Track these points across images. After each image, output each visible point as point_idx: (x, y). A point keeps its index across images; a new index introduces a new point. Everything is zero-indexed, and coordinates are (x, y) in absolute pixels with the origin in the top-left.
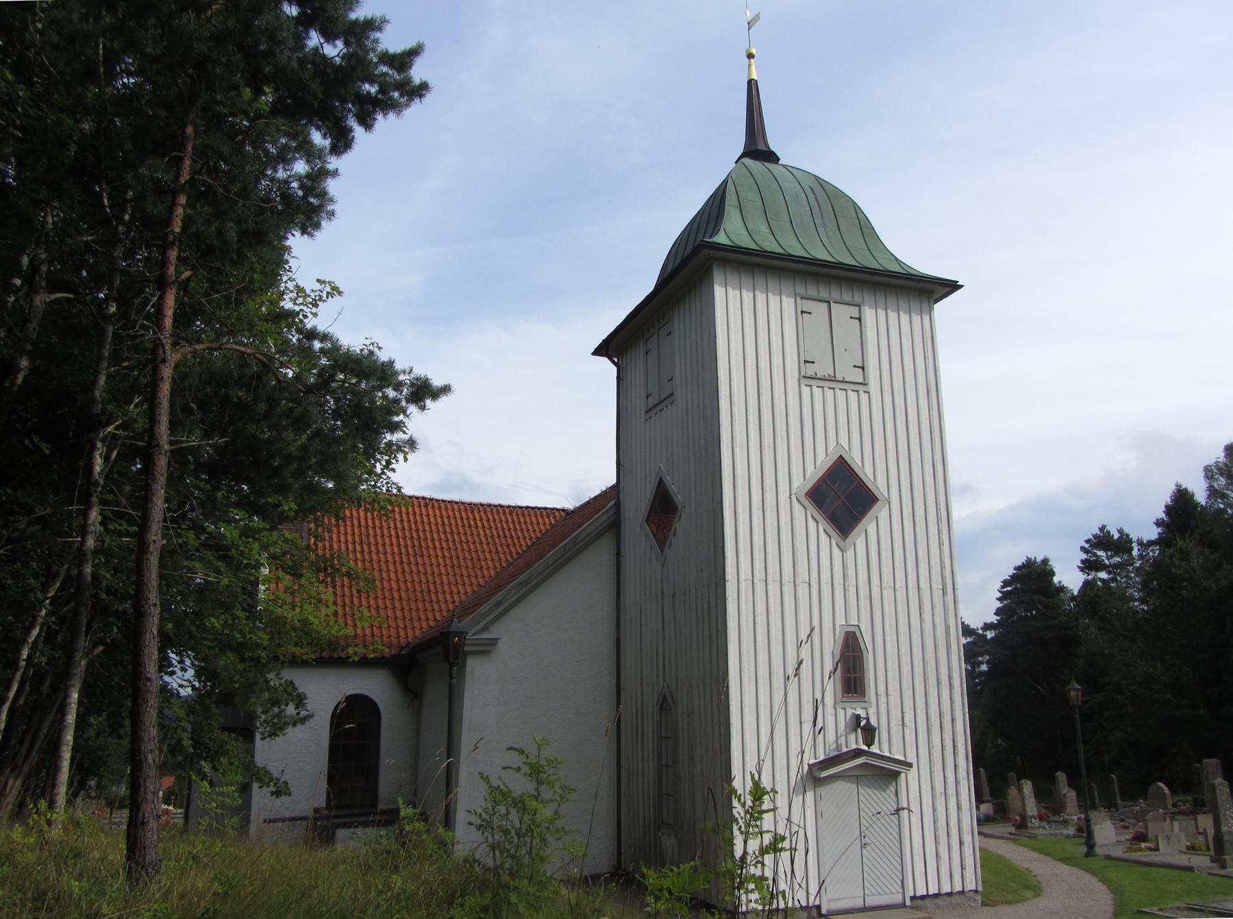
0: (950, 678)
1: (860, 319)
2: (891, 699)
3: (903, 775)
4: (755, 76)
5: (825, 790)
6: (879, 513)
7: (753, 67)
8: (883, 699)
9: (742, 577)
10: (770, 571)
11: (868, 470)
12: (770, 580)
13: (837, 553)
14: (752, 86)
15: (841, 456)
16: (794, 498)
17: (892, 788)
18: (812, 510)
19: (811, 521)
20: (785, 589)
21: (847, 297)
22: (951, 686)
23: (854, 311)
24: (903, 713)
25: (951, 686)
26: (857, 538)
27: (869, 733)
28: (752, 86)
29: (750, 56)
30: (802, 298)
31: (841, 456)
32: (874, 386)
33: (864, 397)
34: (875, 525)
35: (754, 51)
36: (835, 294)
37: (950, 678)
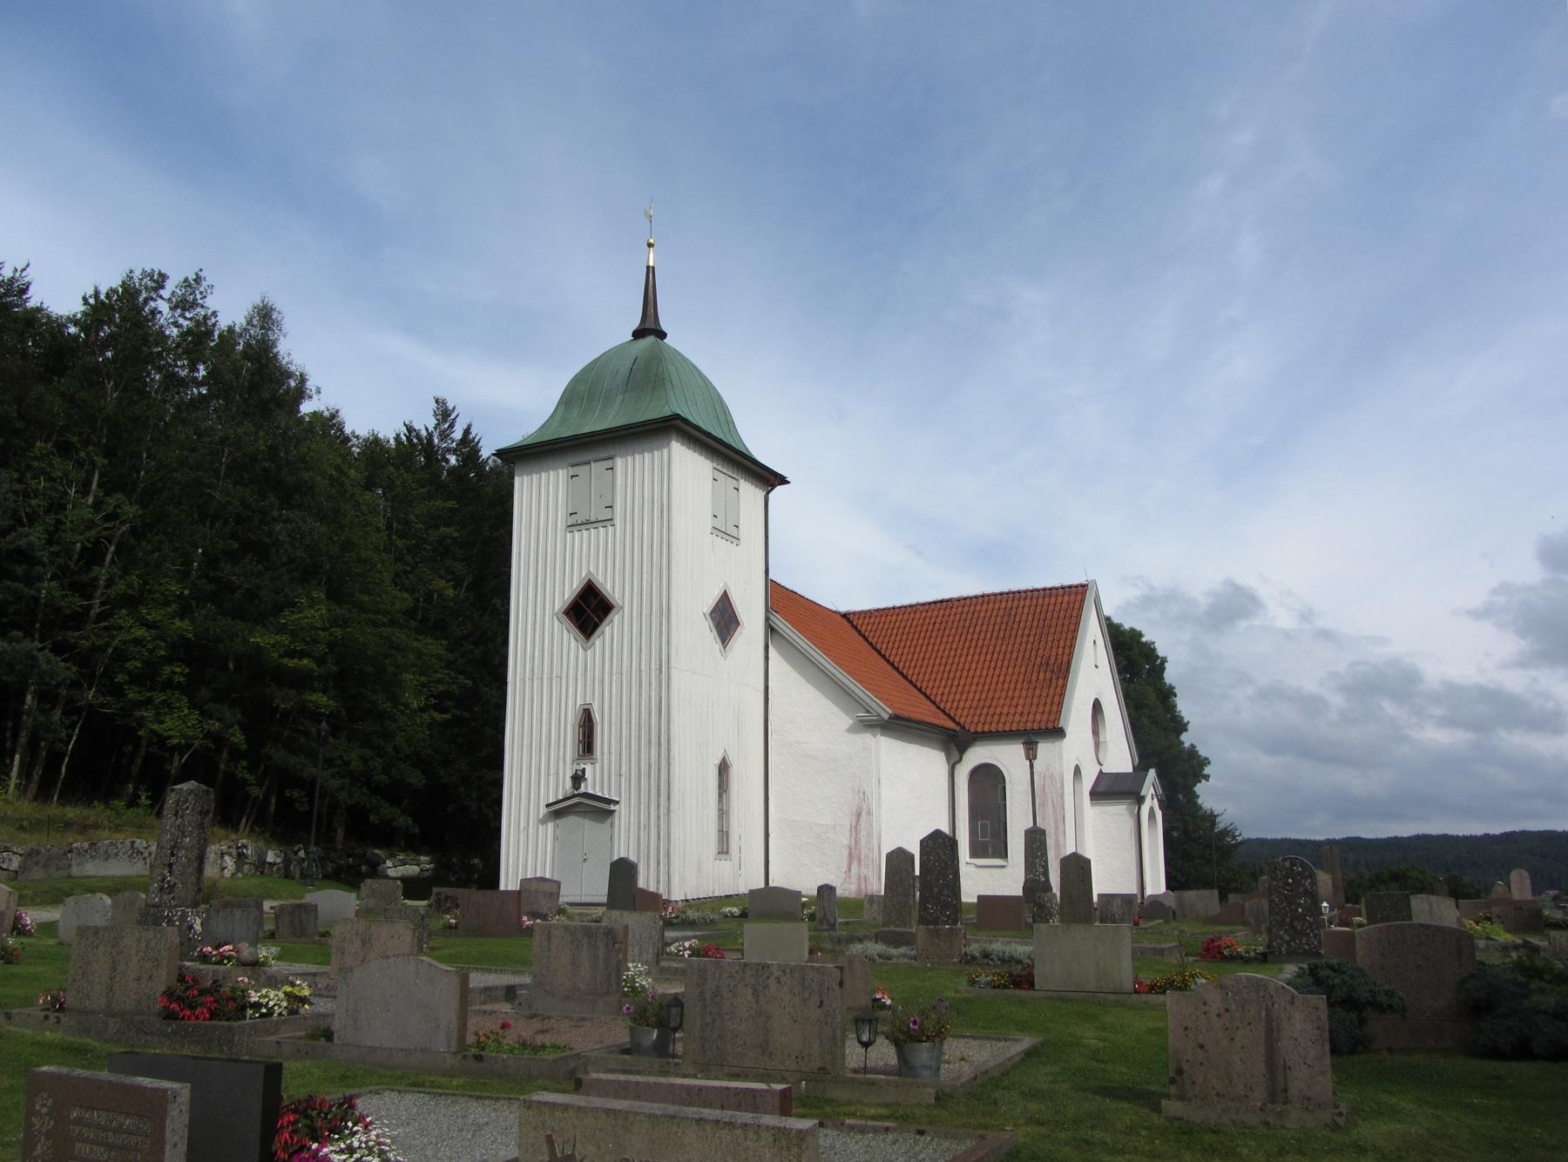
0: (659, 738)
1: (612, 469)
2: (613, 756)
3: (617, 813)
4: (651, 264)
5: (563, 822)
6: (615, 617)
7: (651, 255)
8: (606, 756)
9: (518, 678)
10: (536, 671)
11: (609, 587)
12: (535, 678)
13: (581, 649)
14: (650, 271)
15: (590, 580)
16: (555, 617)
17: (609, 821)
18: (568, 623)
19: (565, 631)
20: (545, 683)
21: (603, 455)
22: (659, 745)
23: (608, 464)
24: (620, 766)
25: (659, 745)
26: (597, 640)
27: (578, 779)
28: (650, 271)
29: (650, 245)
30: (573, 466)
31: (590, 580)
32: (618, 521)
33: (610, 529)
34: (611, 629)
35: (652, 241)
36: (595, 455)
37: (659, 738)
